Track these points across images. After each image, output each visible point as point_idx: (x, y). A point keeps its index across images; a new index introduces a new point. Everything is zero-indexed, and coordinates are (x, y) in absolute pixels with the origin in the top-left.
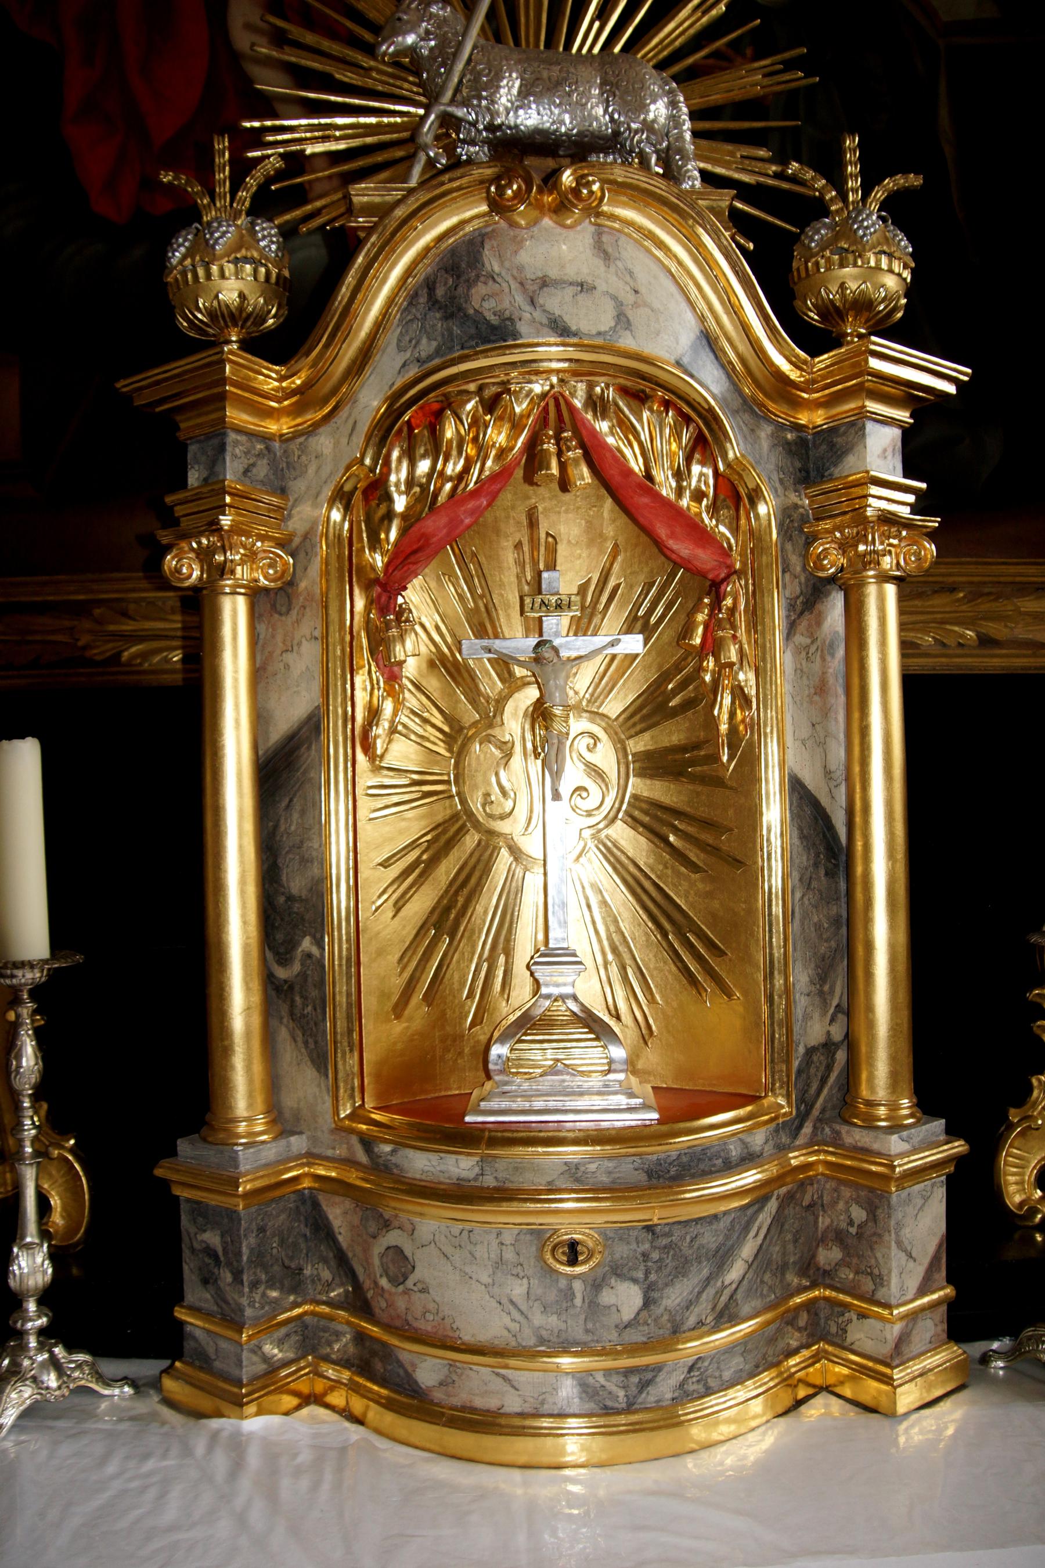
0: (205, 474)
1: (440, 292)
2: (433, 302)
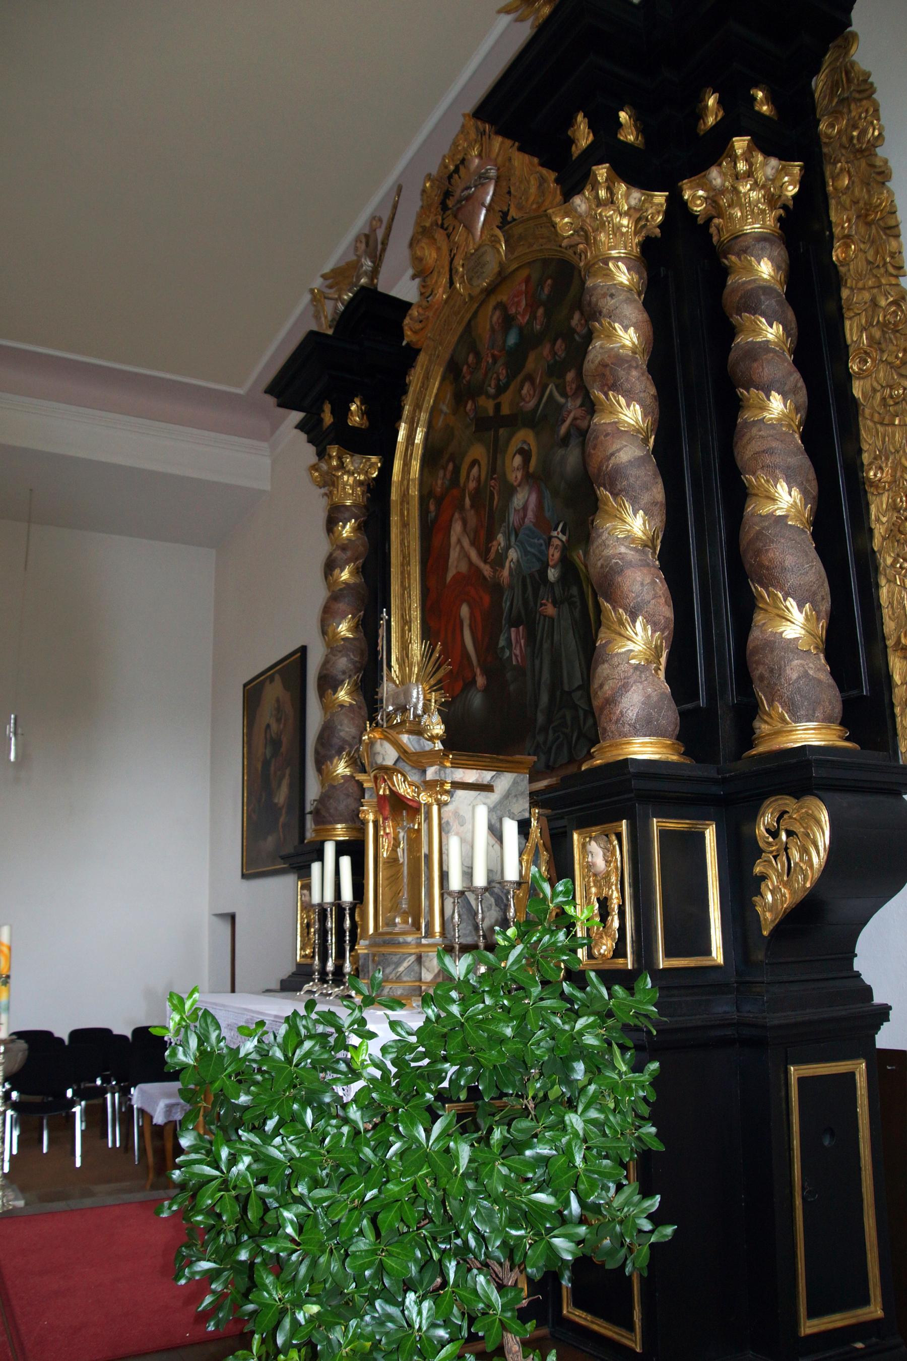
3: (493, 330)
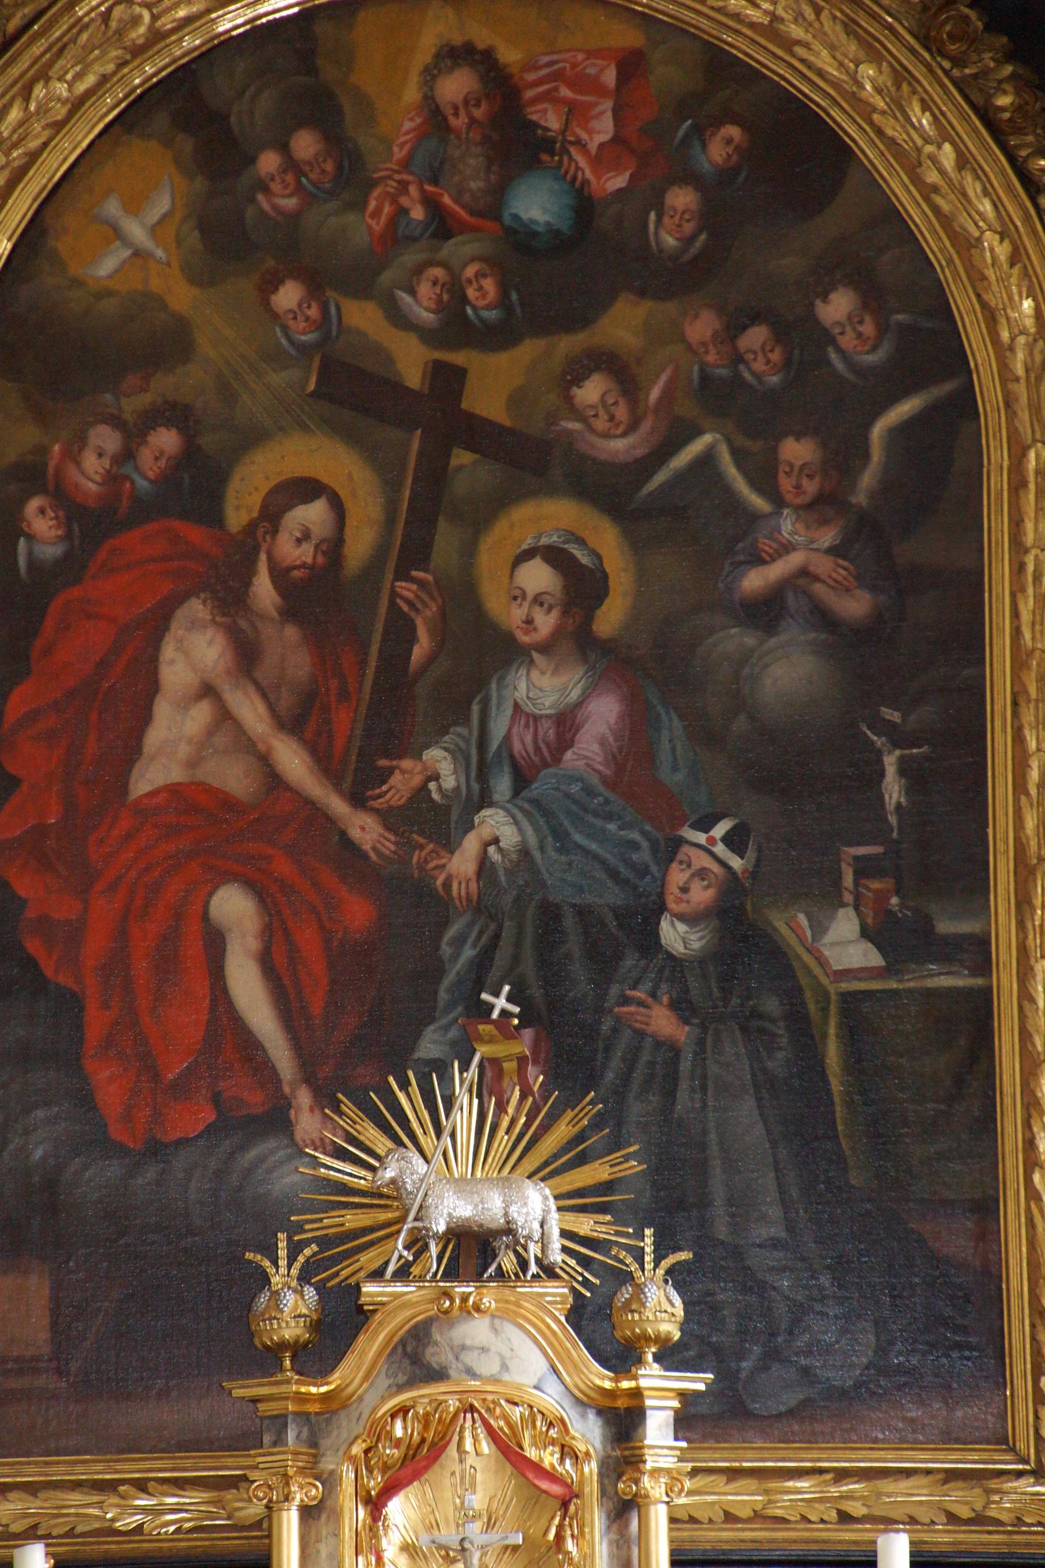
0: (274, 1438)
1: (409, 1349)
2: (405, 1353)
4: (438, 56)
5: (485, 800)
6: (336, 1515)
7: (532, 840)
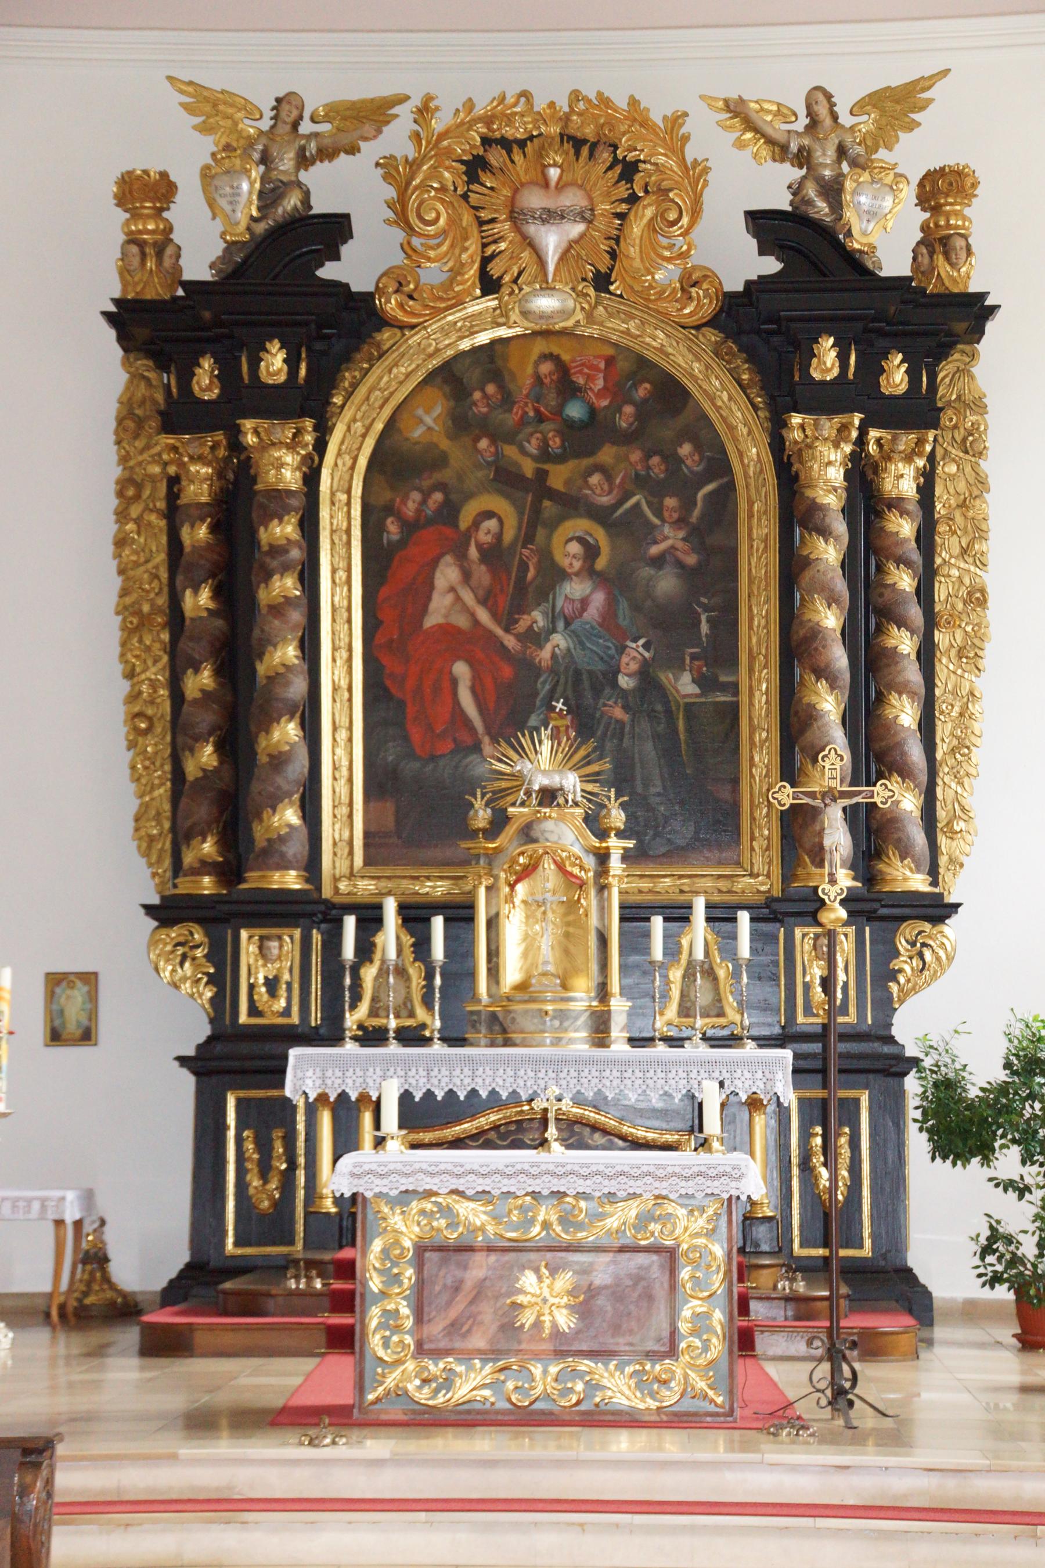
3: (538, 380)
4: (540, 357)
5: (554, 630)
6: (498, 890)
7: (572, 646)
